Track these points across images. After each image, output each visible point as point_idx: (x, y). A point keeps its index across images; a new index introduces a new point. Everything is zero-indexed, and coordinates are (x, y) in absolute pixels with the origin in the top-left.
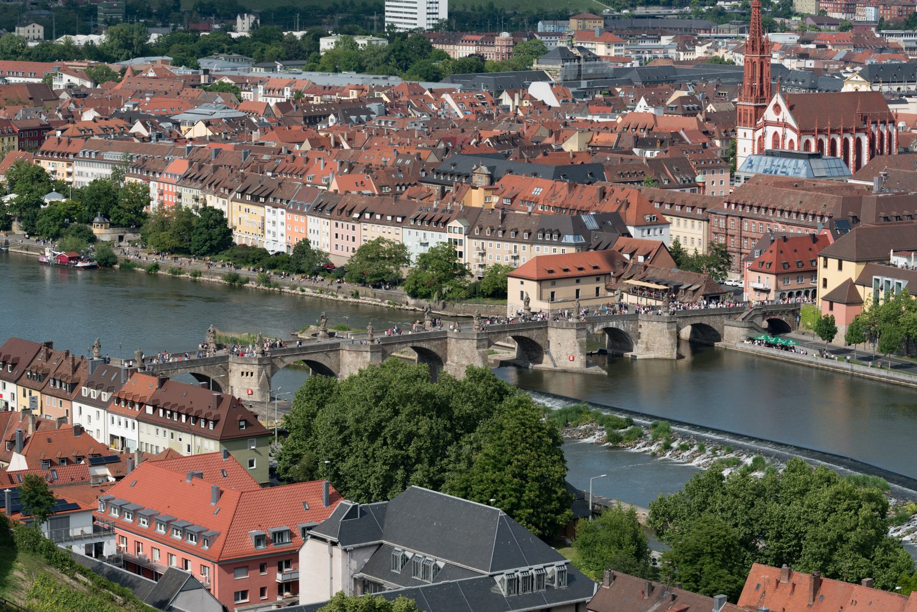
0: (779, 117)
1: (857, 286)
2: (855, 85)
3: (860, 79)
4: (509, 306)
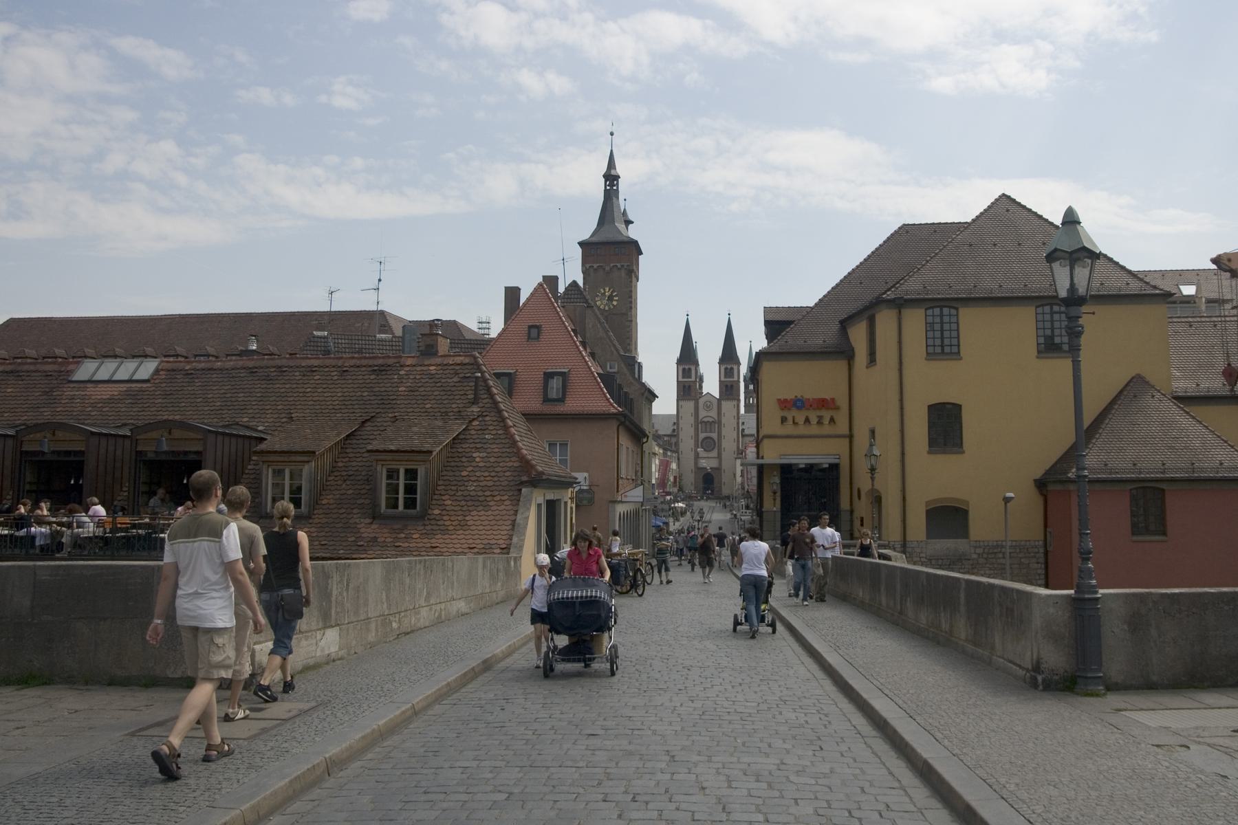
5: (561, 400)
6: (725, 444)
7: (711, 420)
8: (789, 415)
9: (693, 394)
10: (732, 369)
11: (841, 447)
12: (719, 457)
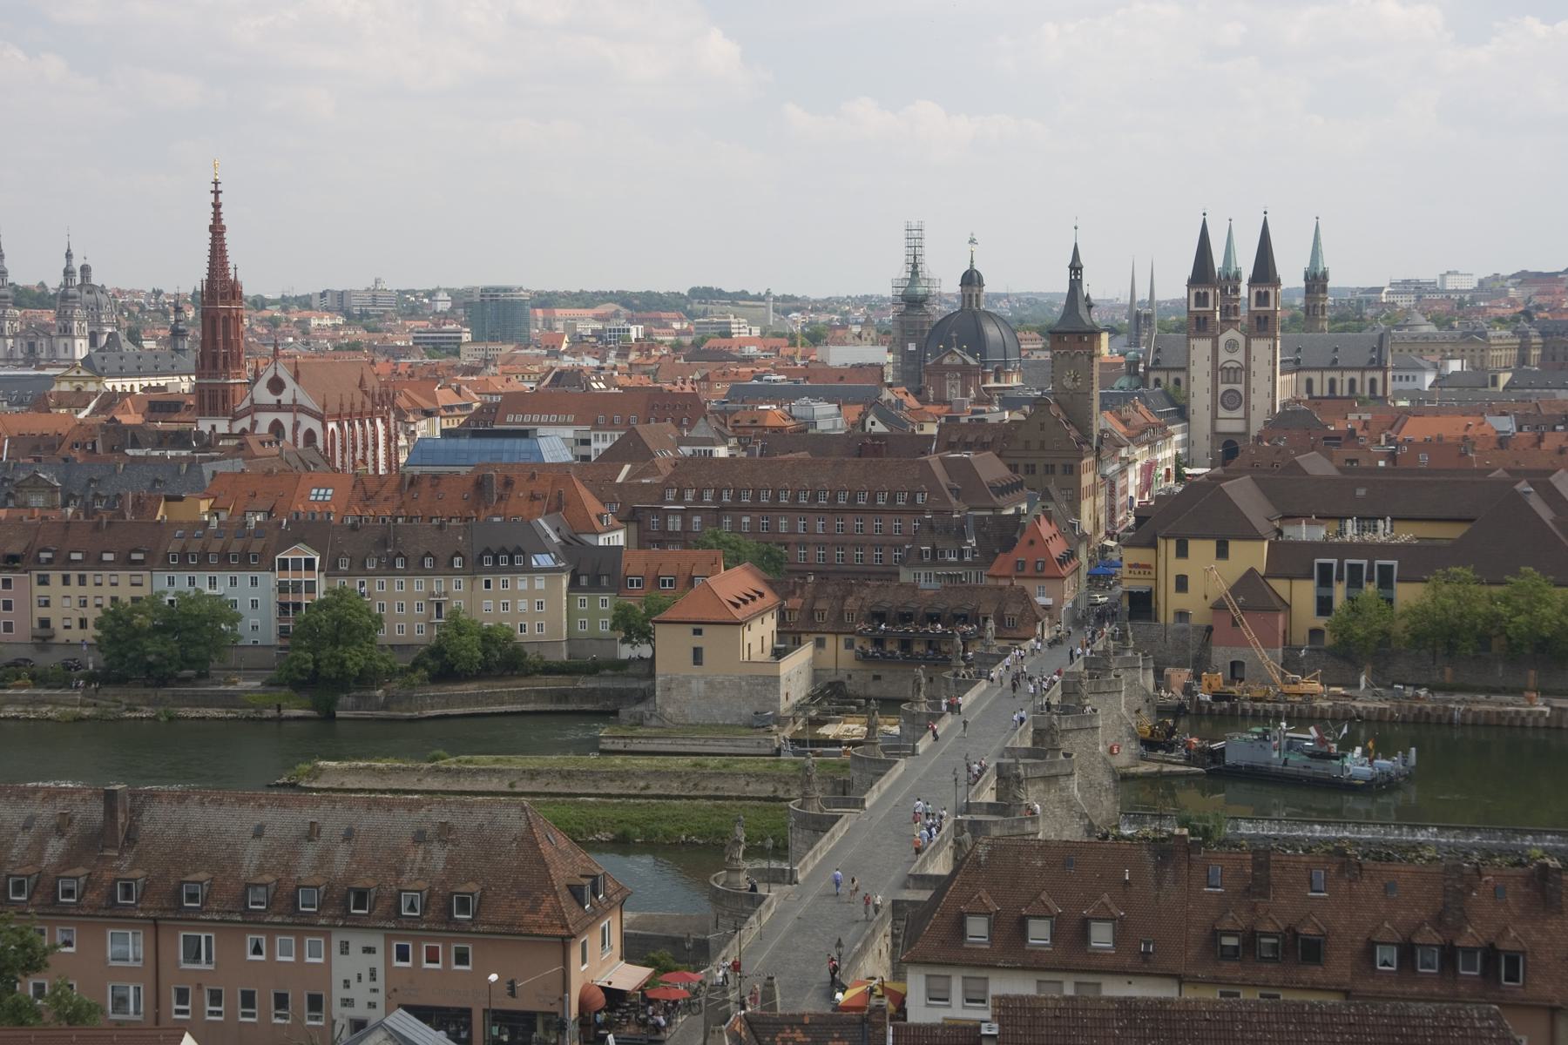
0: (279, 397)
1: (1269, 581)
2: (75, 384)
3: (83, 373)
4: (659, 680)
5: (1043, 570)
6: (1253, 401)
7: (1235, 365)
8: (1133, 570)
9: (1210, 329)
10: (1267, 294)
11: (1151, 584)
12: (1247, 417)
